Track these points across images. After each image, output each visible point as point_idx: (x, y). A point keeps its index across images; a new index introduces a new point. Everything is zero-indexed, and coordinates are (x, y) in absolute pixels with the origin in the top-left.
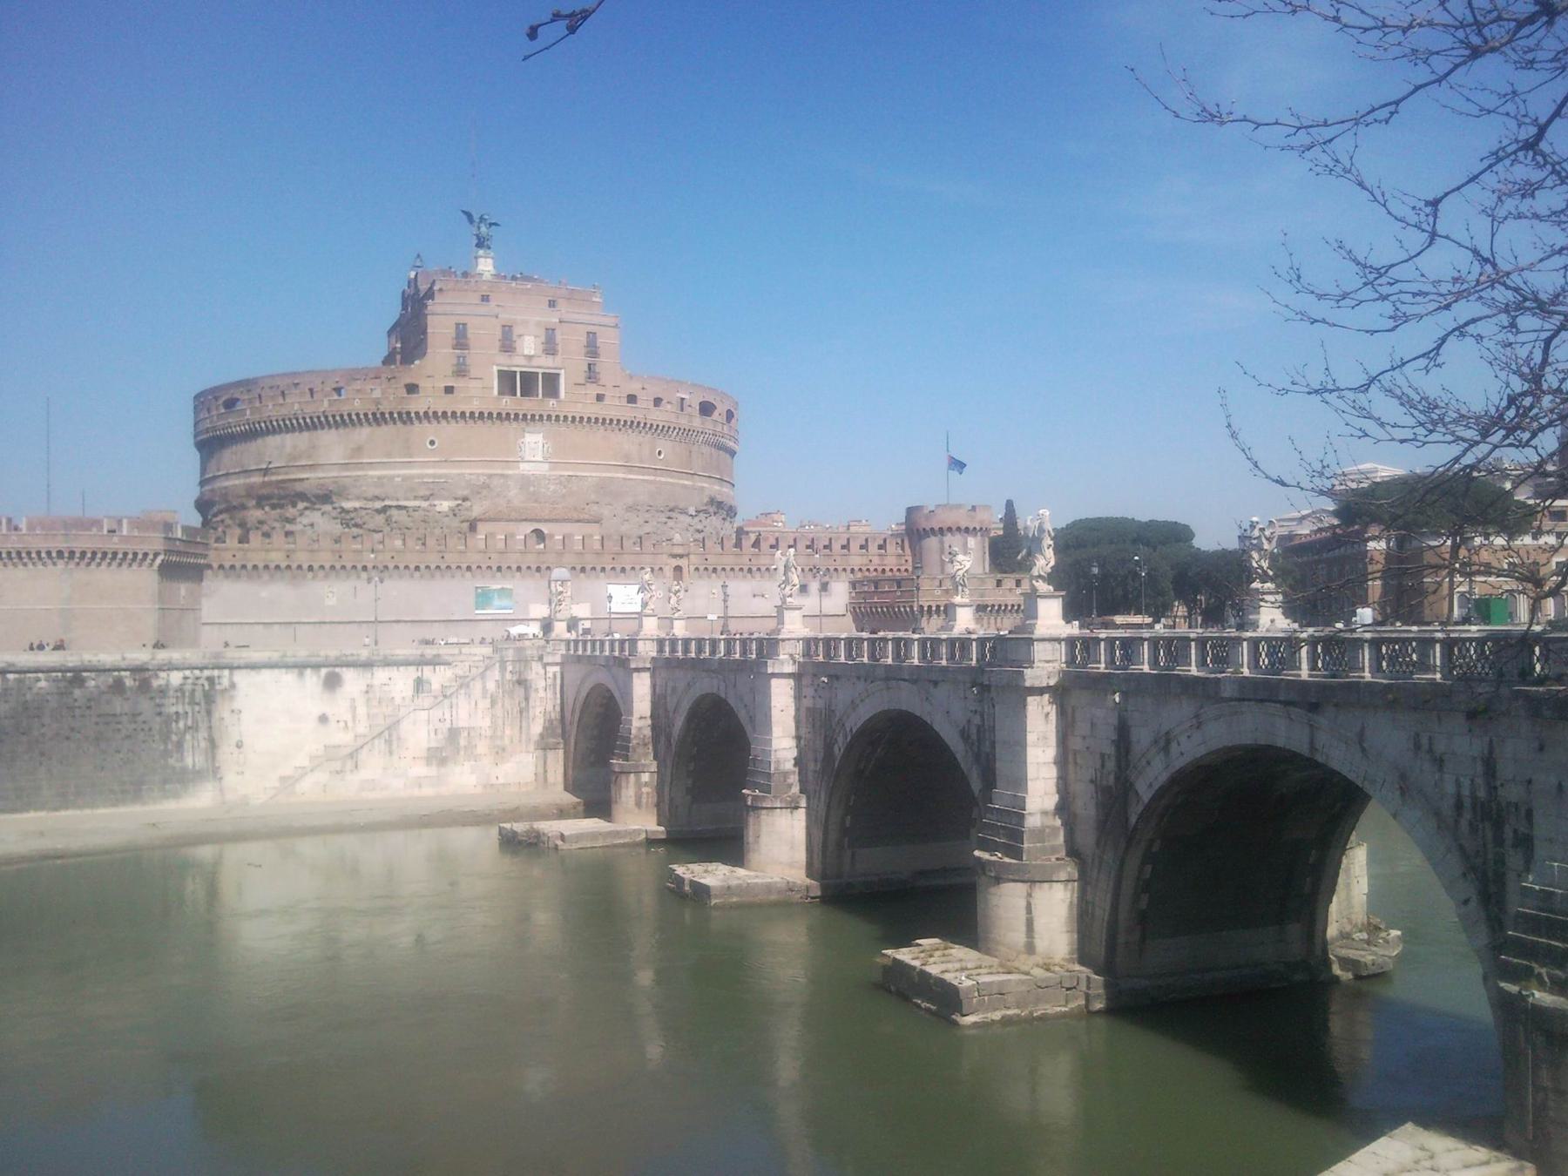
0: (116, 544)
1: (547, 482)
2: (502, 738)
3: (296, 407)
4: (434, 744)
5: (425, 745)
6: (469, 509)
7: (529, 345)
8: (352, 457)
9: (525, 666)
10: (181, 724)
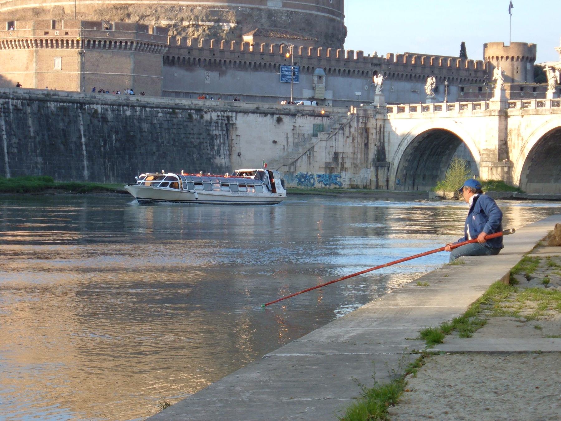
0: (152, 40)
2: (357, 159)
4: (328, 161)
5: (324, 160)
6: (241, 29)
9: (368, 120)
10: (218, 141)
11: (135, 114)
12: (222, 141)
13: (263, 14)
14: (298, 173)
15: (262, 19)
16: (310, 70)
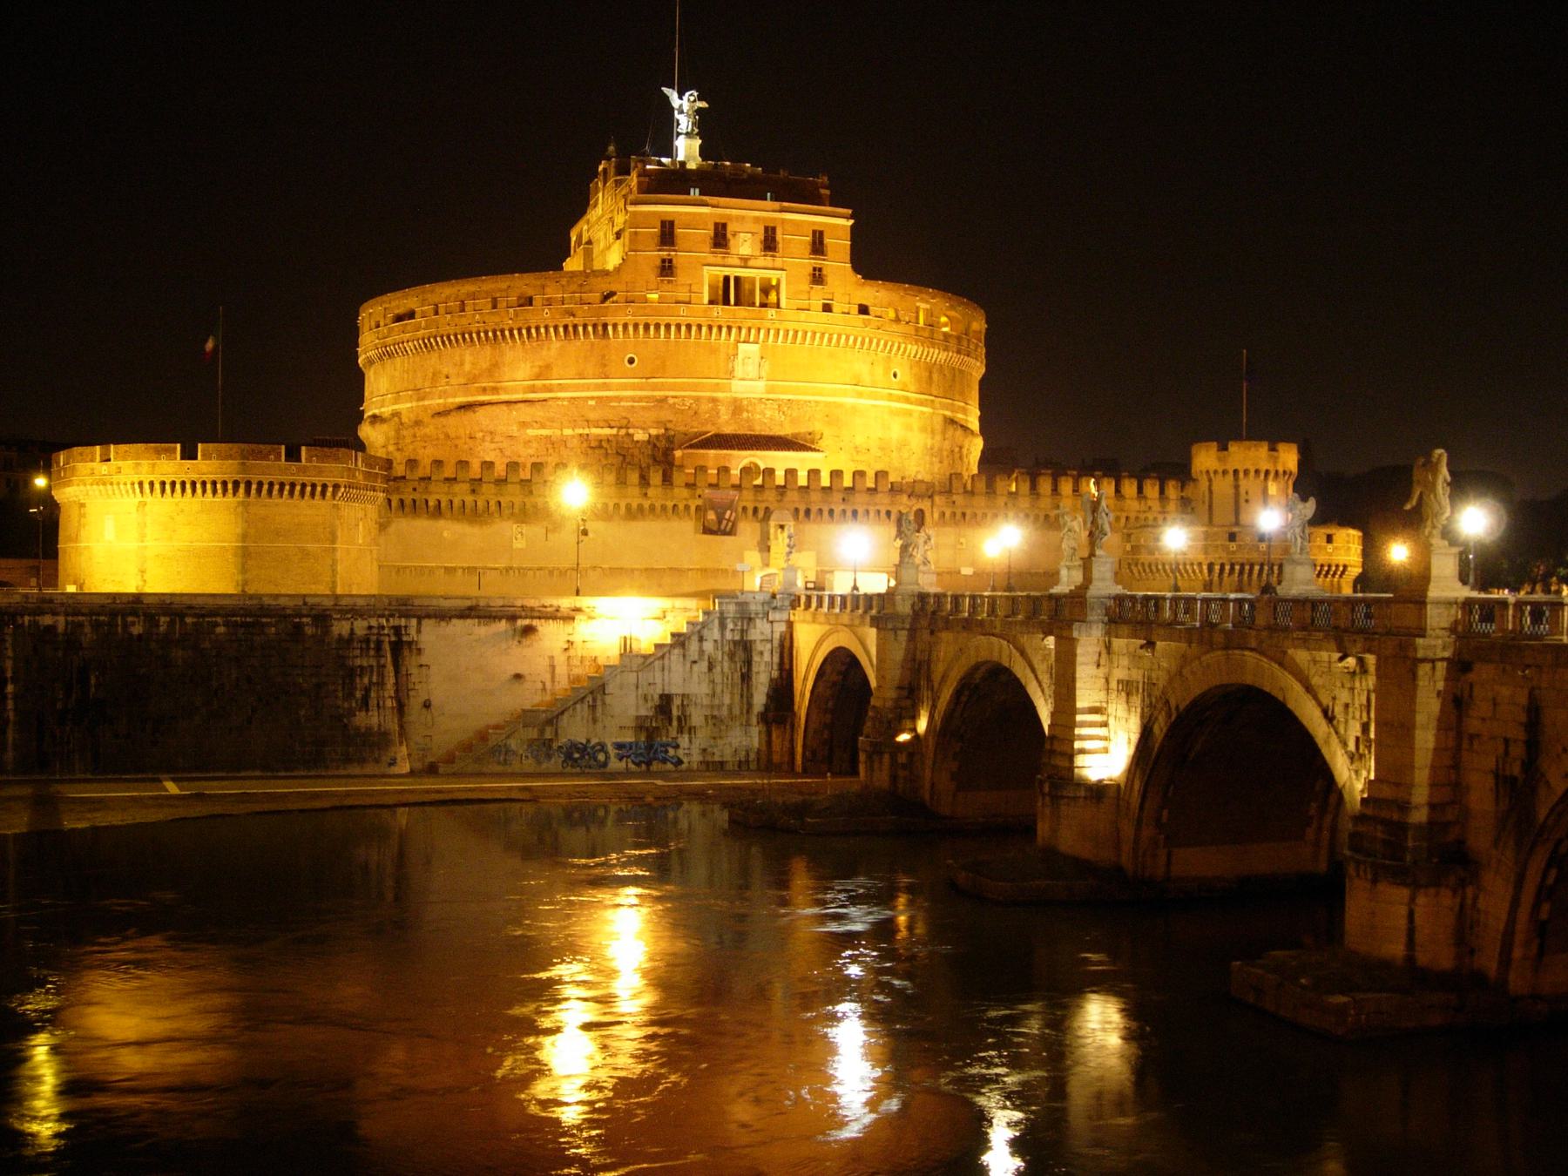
1: (763, 406)
2: (719, 707)
3: (477, 316)
4: (643, 712)
5: (632, 712)
7: (745, 244)
8: (537, 378)
9: (748, 624)
10: (366, 680)
11: (155, 630)
12: (374, 679)
13: (723, 409)
14: (563, 740)
15: (719, 418)
16: (761, 514)
